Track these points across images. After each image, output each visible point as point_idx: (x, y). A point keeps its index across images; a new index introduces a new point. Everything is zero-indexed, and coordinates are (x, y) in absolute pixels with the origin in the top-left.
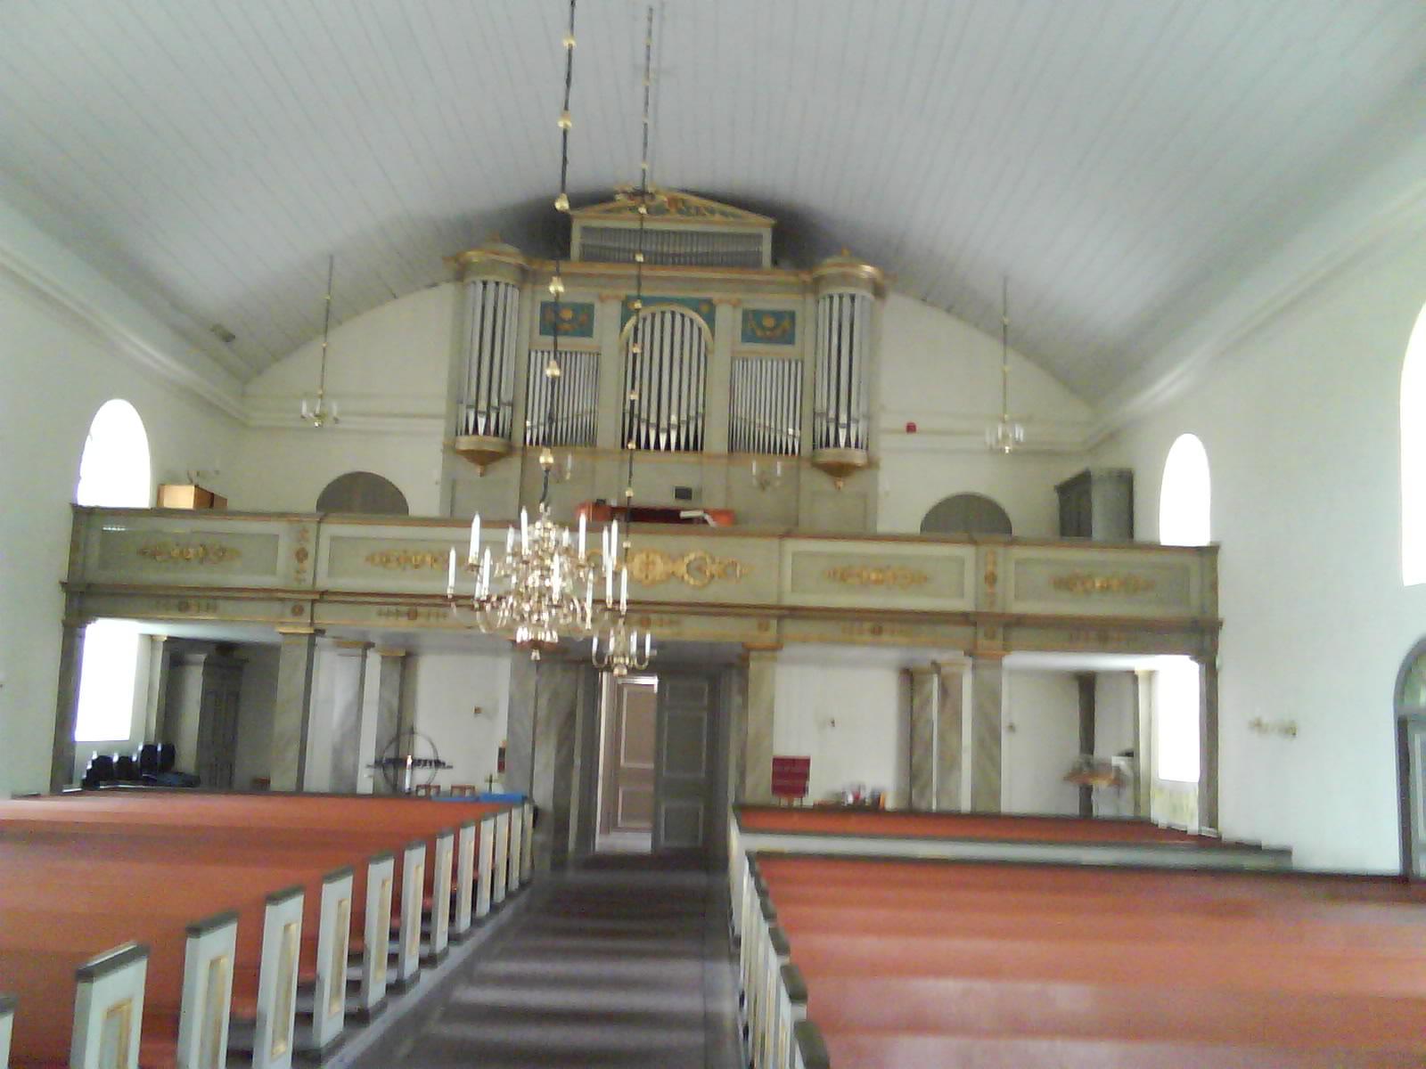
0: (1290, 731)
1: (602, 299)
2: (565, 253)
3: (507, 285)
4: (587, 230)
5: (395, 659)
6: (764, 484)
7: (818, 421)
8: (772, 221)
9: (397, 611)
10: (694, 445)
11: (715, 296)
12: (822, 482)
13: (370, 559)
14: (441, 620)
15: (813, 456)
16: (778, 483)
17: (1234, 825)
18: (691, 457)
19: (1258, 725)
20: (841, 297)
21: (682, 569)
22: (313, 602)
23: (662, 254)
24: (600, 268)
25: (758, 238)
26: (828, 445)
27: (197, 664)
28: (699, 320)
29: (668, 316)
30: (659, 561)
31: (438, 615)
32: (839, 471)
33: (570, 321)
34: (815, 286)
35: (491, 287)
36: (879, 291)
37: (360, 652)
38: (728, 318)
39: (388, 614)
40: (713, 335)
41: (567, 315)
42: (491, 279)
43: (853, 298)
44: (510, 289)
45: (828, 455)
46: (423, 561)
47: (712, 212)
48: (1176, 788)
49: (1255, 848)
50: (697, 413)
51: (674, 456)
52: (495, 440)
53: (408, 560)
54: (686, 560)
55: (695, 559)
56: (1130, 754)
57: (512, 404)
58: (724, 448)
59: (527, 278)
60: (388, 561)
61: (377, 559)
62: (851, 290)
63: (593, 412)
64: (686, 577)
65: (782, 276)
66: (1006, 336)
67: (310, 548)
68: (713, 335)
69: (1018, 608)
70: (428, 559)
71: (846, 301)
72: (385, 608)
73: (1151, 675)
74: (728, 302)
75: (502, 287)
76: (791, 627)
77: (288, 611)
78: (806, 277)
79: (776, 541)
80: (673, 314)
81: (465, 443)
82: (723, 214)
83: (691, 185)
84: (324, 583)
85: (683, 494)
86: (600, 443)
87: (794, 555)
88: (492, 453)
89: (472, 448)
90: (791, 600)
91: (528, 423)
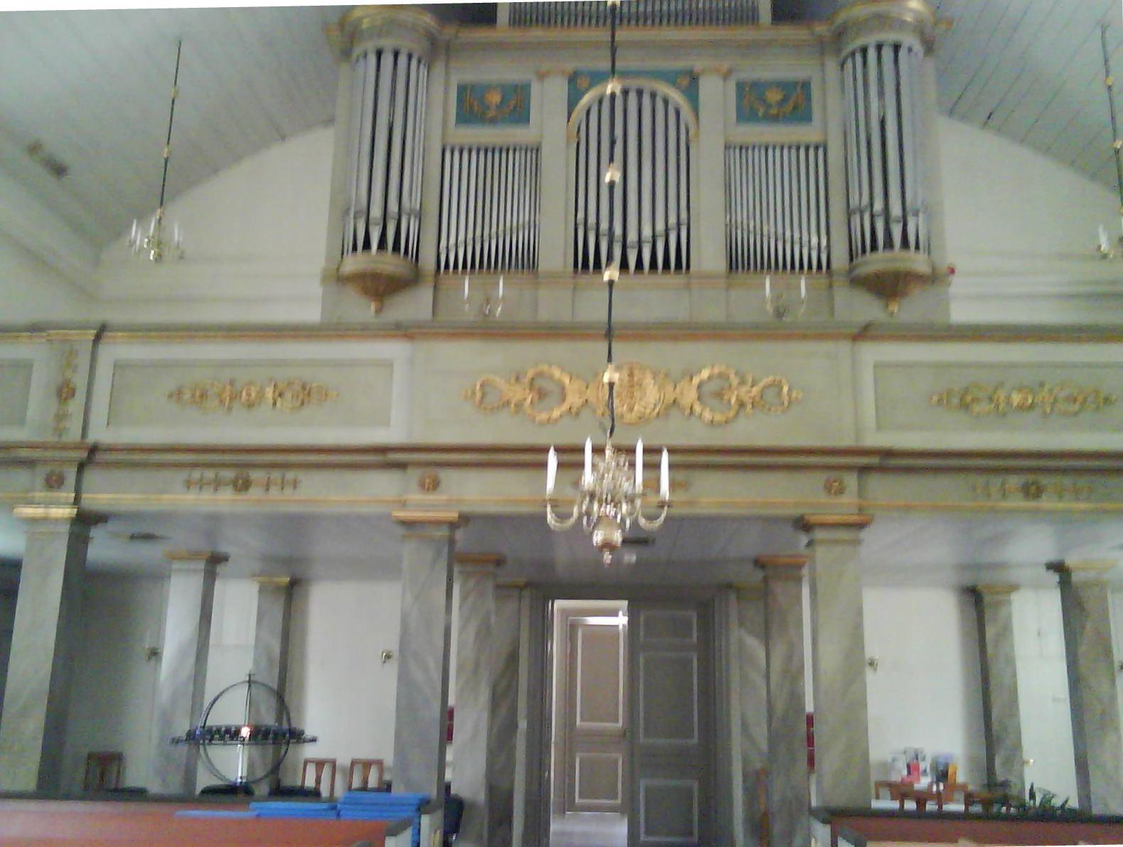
1: (542, 76)
5: (278, 588)
11: (698, 65)
13: (177, 395)
14: (288, 491)
15: (851, 270)
18: (673, 279)
20: (879, 47)
21: (689, 396)
22: (81, 467)
26: (874, 247)
28: (676, 97)
30: (649, 381)
35: (387, 60)
37: (201, 566)
38: (717, 94)
39: (201, 484)
43: (897, 48)
45: (877, 262)
46: (261, 395)
54: (696, 381)
55: (710, 378)
58: (721, 264)
61: (187, 396)
62: (890, 37)
63: (534, 226)
65: (788, 32)
67: (80, 381)
70: (269, 392)
71: (887, 54)
72: (196, 474)
74: (717, 71)
76: (882, 489)
77: (40, 481)
78: (821, 29)
79: (844, 348)
81: (354, 263)
84: (100, 433)
86: (544, 264)
87: (878, 366)
90: (875, 440)
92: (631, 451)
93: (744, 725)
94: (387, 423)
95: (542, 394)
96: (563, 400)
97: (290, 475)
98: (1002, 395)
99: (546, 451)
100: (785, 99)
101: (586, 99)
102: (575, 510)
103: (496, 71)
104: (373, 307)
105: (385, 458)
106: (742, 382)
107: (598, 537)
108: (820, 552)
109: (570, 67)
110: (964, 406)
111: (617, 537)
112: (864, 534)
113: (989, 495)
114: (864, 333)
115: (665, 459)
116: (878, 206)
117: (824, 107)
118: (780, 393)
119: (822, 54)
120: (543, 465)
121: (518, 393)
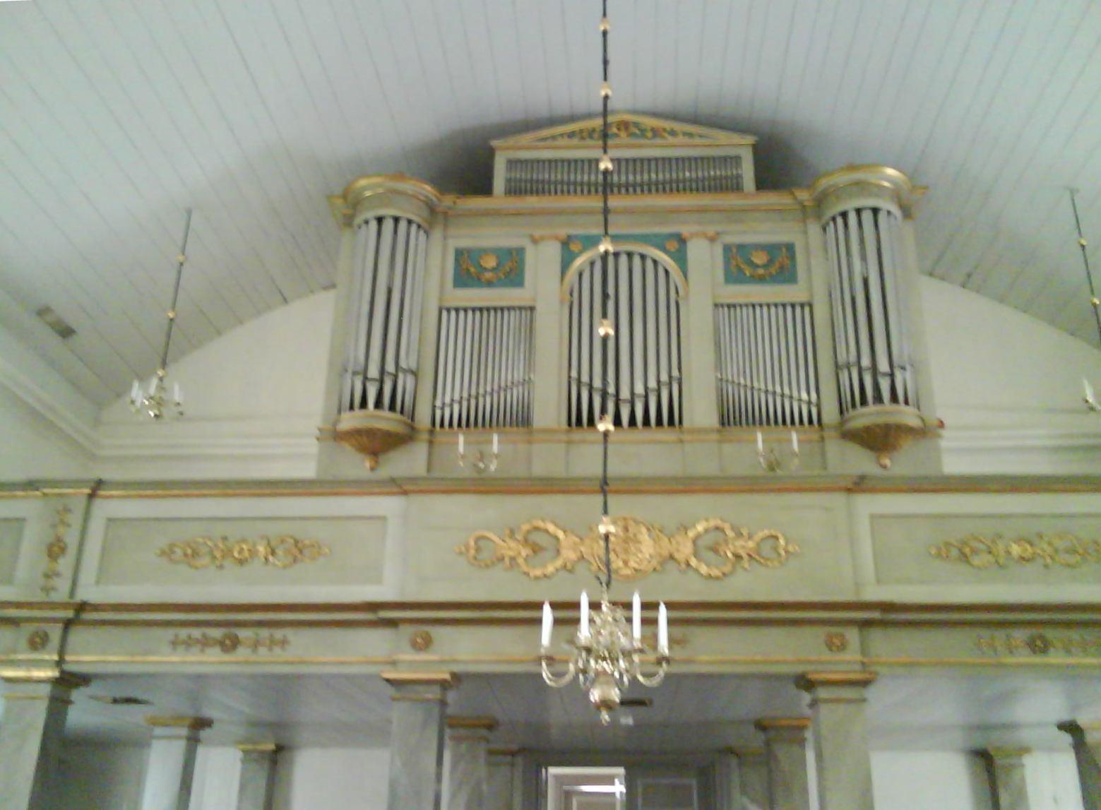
2: (485, 189)
3: (410, 222)
4: (512, 164)
7: (844, 376)
8: (750, 140)
9: (204, 636)
10: (671, 418)
11: (685, 230)
13: (168, 553)
14: (277, 650)
15: (843, 422)
18: (666, 434)
20: (858, 211)
21: (685, 550)
22: (68, 624)
24: (532, 202)
25: (737, 160)
26: (864, 402)
30: (644, 536)
31: (273, 643)
33: (493, 269)
35: (388, 225)
37: (184, 732)
39: (189, 643)
41: (490, 262)
43: (875, 211)
44: (414, 228)
46: (253, 553)
47: (673, 133)
50: (670, 377)
53: (227, 553)
54: (691, 534)
55: (707, 531)
57: (415, 374)
58: (712, 420)
59: (434, 217)
60: (195, 554)
61: (179, 552)
62: (872, 202)
63: (527, 382)
64: (693, 562)
65: (771, 199)
67: (71, 539)
70: (261, 549)
71: (867, 217)
72: (183, 633)
74: (705, 235)
75: (403, 225)
76: (886, 645)
77: (23, 643)
78: (803, 195)
79: (838, 499)
81: (350, 421)
83: (645, 102)
84: (88, 593)
87: (873, 517)
88: (388, 434)
90: (873, 593)
91: (438, 403)
92: (628, 606)
94: (378, 580)
95: (536, 549)
97: (279, 634)
98: (1001, 546)
99: (538, 606)
100: (770, 262)
101: (579, 262)
102: (572, 667)
103: (490, 237)
104: (368, 464)
105: (377, 615)
106: (739, 535)
107: (595, 695)
108: (824, 710)
109: (563, 232)
110: (964, 558)
111: (615, 695)
112: (871, 693)
113: (995, 651)
114: (859, 485)
115: (663, 614)
116: (866, 362)
117: (809, 270)
118: (775, 549)
119: (804, 221)
120: (538, 622)
121: (512, 548)
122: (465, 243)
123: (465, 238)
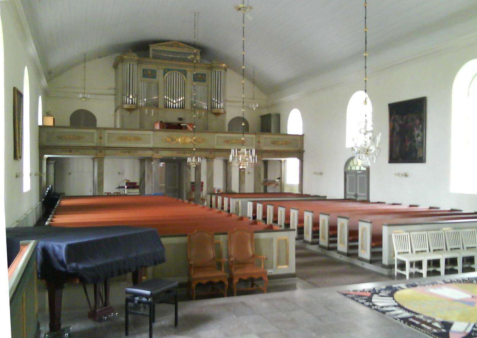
0: (321, 174)
4: (154, 50)
6: (199, 117)
12: (213, 116)
16: (203, 117)
17: (305, 192)
18: (181, 110)
19: (315, 173)
20: (218, 72)
23: (173, 58)
24: (159, 61)
27: (52, 163)
29: (175, 74)
32: (217, 114)
34: (211, 68)
36: (226, 70)
38: (190, 75)
40: (186, 79)
42: (132, 63)
43: (221, 72)
45: (215, 111)
48: (291, 186)
49: (319, 196)
51: (178, 110)
52: (134, 105)
56: (279, 179)
66: (254, 82)
68: (186, 79)
69: (265, 148)
72: (123, 151)
73: (285, 161)
76: (217, 153)
80: (176, 73)
82: (187, 47)
84: (107, 145)
85: (180, 119)
89: (128, 107)
93: (186, 183)
95: (172, 140)
96: (176, 141)
97: (137, 151)
101: (166, 75)
106: (200, 139)
109: (164, 67)
121: (168, 140)
122: (143, 68)
123: (145, 67)
